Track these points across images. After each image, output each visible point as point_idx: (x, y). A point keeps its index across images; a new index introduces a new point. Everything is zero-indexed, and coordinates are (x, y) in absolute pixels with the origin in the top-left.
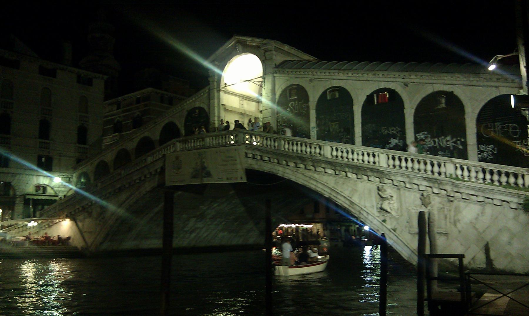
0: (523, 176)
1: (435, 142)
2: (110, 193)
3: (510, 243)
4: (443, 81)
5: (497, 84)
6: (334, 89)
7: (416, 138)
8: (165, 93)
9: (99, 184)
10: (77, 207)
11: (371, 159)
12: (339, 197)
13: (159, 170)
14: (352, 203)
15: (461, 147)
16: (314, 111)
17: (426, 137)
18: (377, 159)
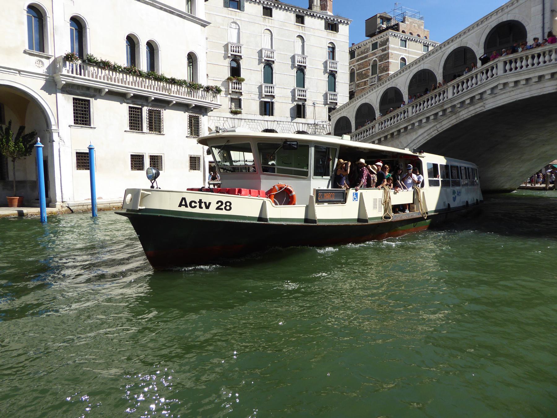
2: (392, 134)
9: (377, 125)
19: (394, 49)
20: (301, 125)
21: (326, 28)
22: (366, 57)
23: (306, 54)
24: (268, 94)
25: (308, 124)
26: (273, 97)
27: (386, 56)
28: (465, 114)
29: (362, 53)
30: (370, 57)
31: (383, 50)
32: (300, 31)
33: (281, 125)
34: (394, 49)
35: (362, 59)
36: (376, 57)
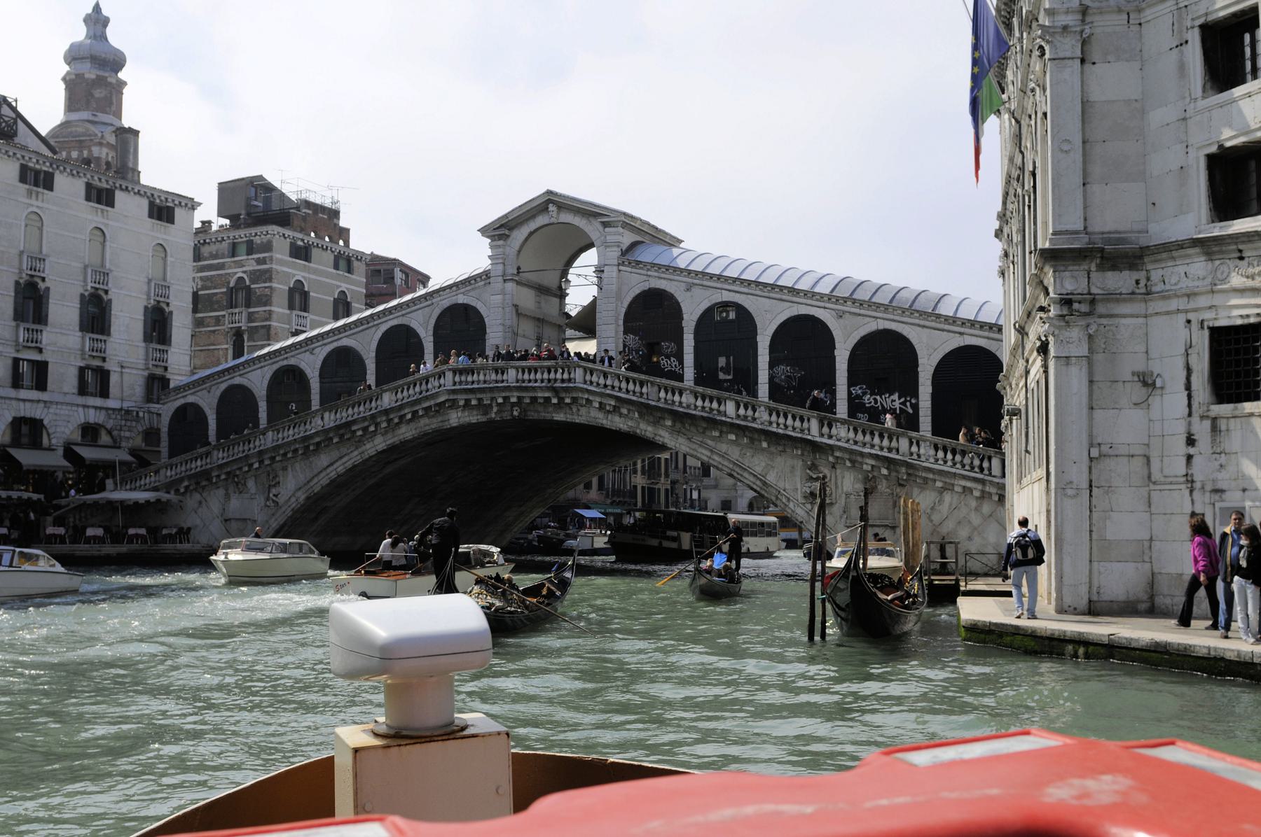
0: (990, 459)
1: (876, 400)
2: (296, 451)
3: (970, 538)
4: (891, 317)
5: (962, 330)
6: (725, 305)
7: (850, 393)
8: (300, 236)
10: (214, 474)
11: (798, 424)
12: (746, 474)
13: (409, 416)
14: (765, 483)
15: (911, 411)
16: (692, 336)
17: (865, 394)
18: (805, 425)
19: (281, 262)
20: (92, 411)
21: (151, 216)
22: (221, 267)
23: (108, 265)
24: (30, 344)
25: (107, 409)
26: (40, 350)
27: (266, 276)
28: (406, 432)
29: (215, 256)
30: (230, 267)
31: (259, 262)
32: (98, 220)
33: (51, 410)
34: (281, 262)
35: (211, 267)
36: (244, 272)
